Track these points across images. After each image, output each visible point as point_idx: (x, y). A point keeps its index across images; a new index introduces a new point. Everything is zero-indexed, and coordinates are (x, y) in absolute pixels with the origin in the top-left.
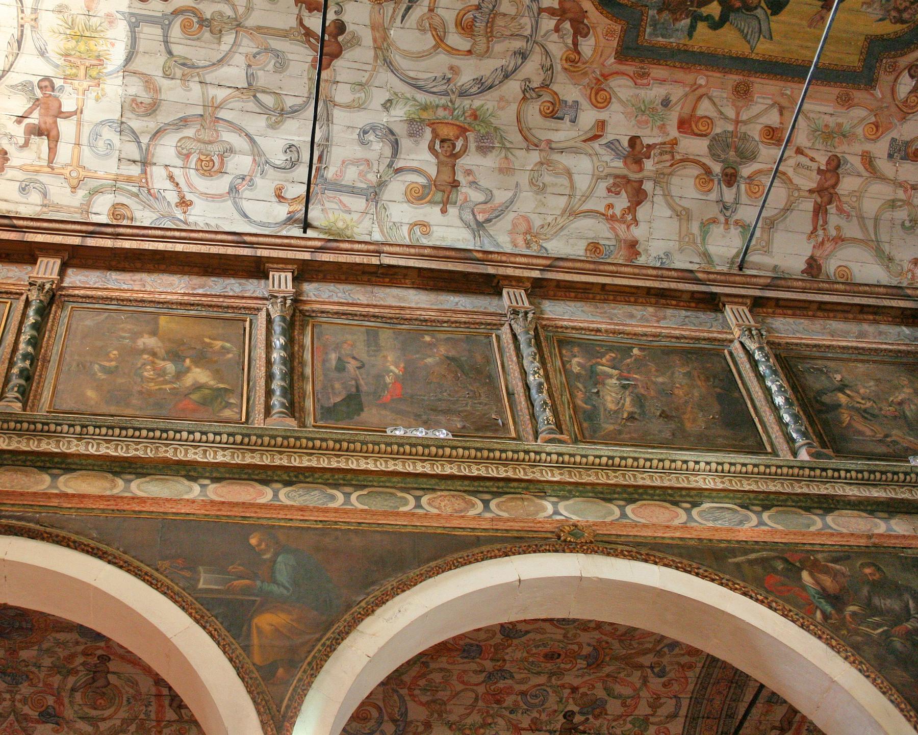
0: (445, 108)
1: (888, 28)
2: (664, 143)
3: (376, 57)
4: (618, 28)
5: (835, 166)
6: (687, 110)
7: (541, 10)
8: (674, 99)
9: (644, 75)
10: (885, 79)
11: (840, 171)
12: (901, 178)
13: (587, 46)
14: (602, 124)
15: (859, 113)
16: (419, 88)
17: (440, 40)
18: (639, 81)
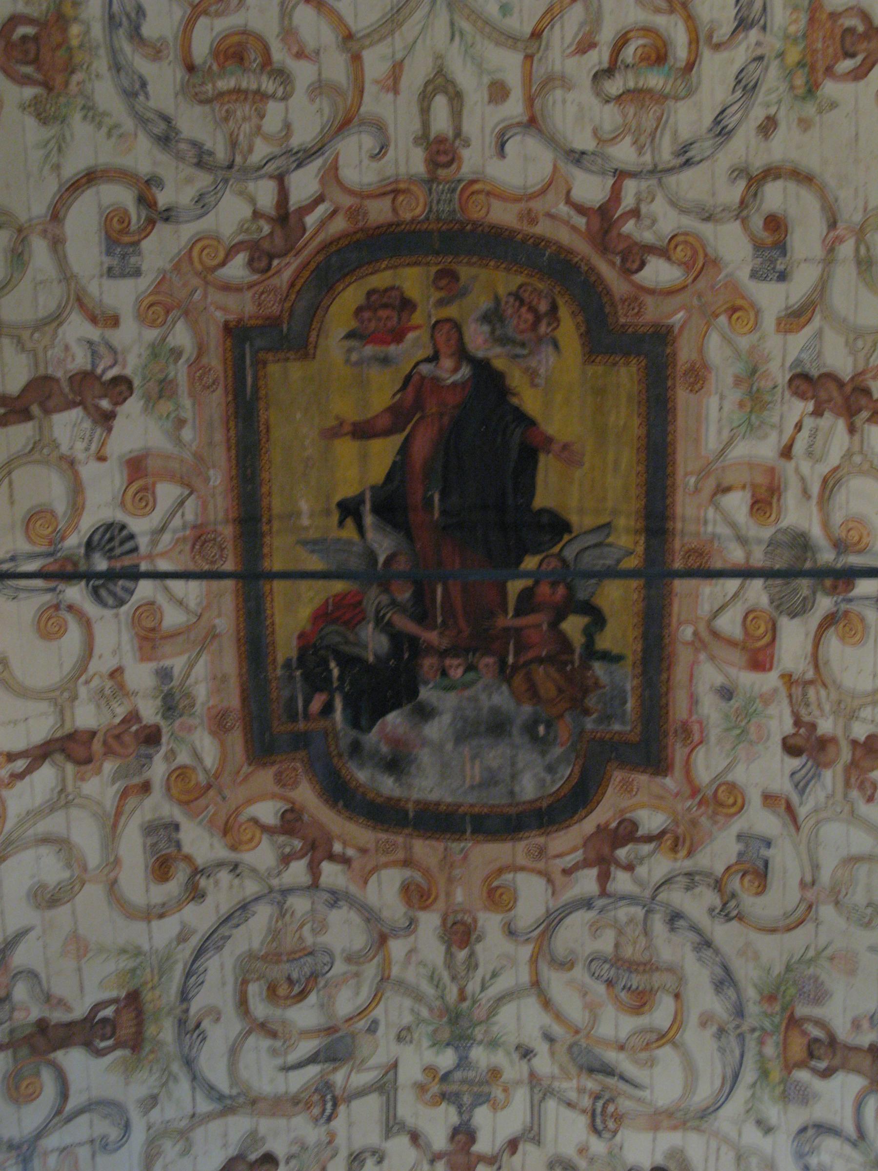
0: (761, 1042)
1: (568, 329)
2: (790, 696)
3: (697, 1129)
4: (618, 775)
5: (804, 382)
6: (737, 656)
7: (604, 893)
8: (719, 680)
9: (686, 730)
10: (653, 311)
11: (815, 373)
12: (818, 252)
13: (651, 821)
14: (769, 799)
15: (715, 349)
16: (736, 1076)
17: (663, 1038)
18: (696, 737)
